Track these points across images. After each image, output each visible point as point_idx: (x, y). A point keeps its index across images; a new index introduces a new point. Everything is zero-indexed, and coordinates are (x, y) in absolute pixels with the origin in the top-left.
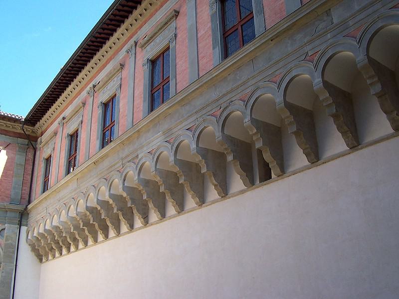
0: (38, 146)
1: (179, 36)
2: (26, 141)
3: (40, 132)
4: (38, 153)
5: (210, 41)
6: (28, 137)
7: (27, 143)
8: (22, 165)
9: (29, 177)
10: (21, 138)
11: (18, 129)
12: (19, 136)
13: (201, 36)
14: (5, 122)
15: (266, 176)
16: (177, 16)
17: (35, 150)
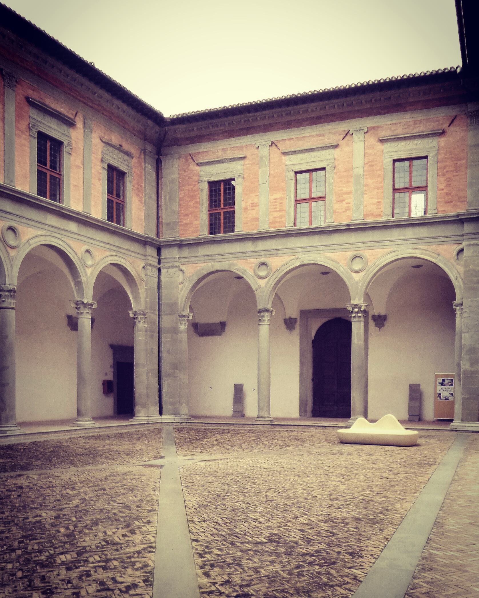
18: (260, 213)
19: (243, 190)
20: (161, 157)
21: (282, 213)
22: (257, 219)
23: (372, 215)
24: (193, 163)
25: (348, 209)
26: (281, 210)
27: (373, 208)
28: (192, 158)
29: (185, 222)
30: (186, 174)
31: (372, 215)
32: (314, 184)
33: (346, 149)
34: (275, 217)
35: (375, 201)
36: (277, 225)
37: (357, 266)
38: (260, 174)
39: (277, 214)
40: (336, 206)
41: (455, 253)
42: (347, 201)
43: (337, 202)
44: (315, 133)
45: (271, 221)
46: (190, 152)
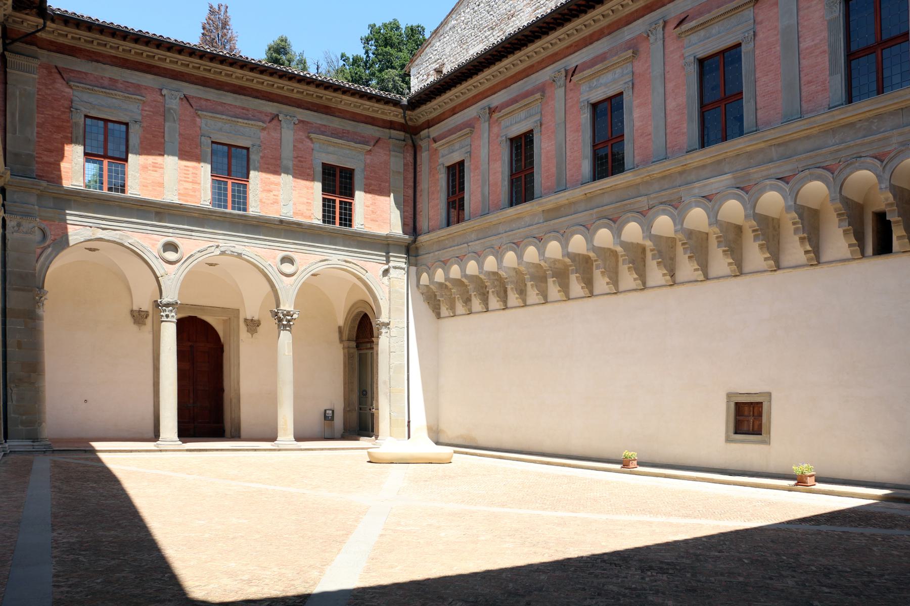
0: (423, 144)
2: (401, 135)
3: (423, 120)
4: (424, 156)
6: (403, 127)
7: (403, 138)
8: (399, 172)
9: (411, 192)
12: (391, 125)
14: (371, 104)
17: (415, 149)
18: (166, 178)
19: (141, 143)
20: (6, 53)
21: (196, 186)
22: (161, 185)
24: (61, 81)
28: (60, 73)
30: (48, 92)
32: (233, 161)
33: (275, 135)
34: (185, 189)
35: (306, 200)
37: (287, 268)
38: (166, 129)
39: (189, 186)
40: (264, 195)
42: (274, 193)
43: (264, 190)
44: (238, 104)
45: (181, 192)
46: (60, 65)
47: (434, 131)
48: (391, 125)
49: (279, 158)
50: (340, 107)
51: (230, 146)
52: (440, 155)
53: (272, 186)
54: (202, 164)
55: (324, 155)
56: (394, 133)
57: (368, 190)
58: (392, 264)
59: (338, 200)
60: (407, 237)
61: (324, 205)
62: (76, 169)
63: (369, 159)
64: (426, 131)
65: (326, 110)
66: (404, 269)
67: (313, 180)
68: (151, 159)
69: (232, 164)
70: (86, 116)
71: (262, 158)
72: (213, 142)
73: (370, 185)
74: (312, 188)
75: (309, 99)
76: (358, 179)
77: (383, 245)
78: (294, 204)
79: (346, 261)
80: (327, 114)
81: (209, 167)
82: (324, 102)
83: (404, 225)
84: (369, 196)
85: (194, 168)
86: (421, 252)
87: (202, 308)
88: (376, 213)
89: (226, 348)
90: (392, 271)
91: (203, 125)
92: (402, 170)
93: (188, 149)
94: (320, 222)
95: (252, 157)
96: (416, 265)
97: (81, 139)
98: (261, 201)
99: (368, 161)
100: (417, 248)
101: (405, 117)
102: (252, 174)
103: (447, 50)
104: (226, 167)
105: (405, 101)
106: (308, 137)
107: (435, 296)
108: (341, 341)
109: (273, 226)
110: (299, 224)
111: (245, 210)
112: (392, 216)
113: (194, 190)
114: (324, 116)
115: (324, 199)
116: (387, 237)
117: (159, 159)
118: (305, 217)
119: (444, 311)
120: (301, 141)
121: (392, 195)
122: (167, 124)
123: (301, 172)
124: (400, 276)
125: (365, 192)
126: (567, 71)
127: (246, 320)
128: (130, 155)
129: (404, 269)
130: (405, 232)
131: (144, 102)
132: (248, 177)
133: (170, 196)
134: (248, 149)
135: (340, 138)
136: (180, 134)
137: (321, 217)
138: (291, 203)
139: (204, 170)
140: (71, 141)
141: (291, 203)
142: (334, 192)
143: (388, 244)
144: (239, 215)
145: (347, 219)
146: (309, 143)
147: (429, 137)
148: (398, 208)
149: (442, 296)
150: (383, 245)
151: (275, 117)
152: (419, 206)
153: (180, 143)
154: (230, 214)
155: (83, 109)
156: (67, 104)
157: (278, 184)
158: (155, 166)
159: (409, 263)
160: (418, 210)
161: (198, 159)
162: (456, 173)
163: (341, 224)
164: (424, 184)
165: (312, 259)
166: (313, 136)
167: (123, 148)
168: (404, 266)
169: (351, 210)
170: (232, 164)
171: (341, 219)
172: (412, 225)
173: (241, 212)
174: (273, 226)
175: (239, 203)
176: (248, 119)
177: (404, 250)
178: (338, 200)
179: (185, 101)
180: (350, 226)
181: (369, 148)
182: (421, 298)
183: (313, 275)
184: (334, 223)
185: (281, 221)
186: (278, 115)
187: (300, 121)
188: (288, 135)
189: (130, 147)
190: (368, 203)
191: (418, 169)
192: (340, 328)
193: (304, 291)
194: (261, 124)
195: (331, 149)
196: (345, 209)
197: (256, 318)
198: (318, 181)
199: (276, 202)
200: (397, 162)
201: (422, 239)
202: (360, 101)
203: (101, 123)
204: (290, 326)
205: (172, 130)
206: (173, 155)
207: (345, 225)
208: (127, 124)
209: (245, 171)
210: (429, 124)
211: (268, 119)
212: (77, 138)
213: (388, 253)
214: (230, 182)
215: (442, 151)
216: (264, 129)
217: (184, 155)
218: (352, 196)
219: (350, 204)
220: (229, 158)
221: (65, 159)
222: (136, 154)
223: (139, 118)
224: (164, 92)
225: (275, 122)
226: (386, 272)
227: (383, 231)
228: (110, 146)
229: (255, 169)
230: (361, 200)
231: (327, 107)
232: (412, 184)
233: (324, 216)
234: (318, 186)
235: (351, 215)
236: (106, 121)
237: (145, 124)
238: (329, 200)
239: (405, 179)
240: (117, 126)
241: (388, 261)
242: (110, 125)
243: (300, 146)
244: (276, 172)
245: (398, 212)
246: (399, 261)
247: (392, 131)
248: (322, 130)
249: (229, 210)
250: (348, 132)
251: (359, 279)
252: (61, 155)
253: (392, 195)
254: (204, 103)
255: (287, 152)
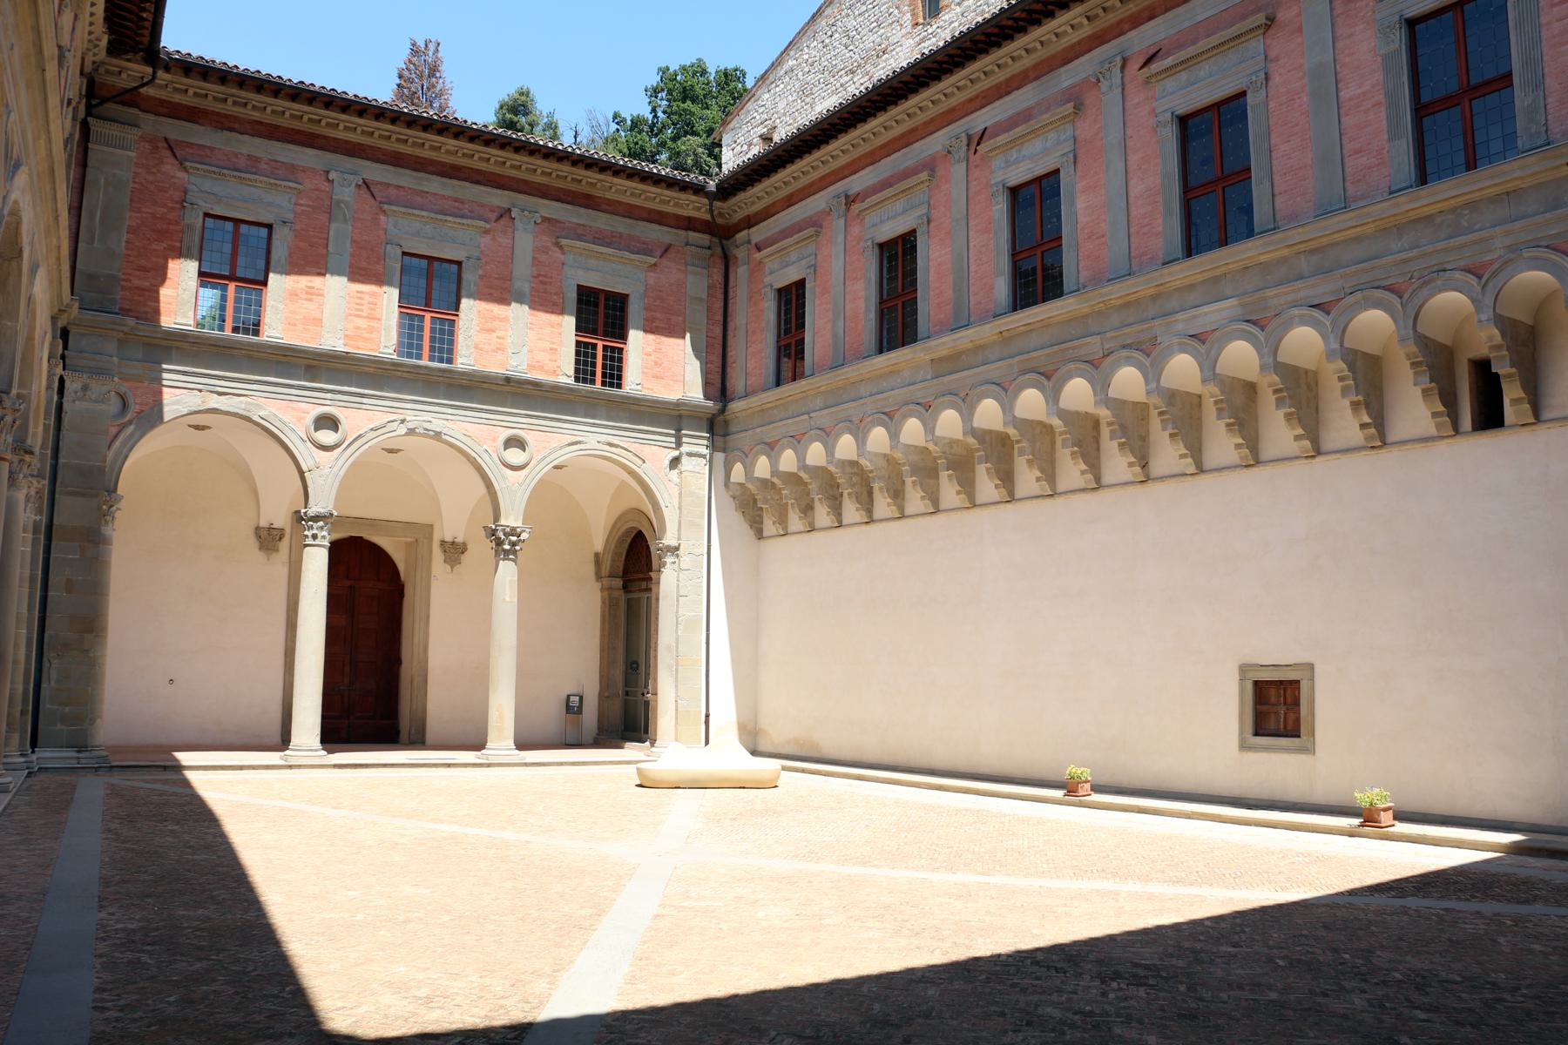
0: (740, 253)
1: (1276, 80)
2: (704, 239)
4: (741, 273)
5: (1380, 118)
6: (708, 227)
7: (707, 243)
8: (701, 299)
9: (718, 331)
10: (695, 230)
11: (693, 207)
12: (689, 224)
13: (1350, 99)
15: (1490, 417)
16: (1268, 27)
17: (727, 261)
19: (290, 255)
22: (318, 322)
23: (541, 368)
25: (501, 349)
26: (370, 318)
27: (543, 357)
29: (137, 282)
31: (541, 368)
32: (436, 284)
33: (503, 240)
35: (548, 345)
36: (361, 344)
37: (515, 456)
41: (667, 462)
42: (499, 333)
47: (758, 233)
48: (689, 224)
49: (509, 278)
50: (608, 196)
51: (431, 259)
52: (767, 271)
53: (496, 323)
54: (385, 288)
55: (580, 272)
56: (693, 236)
57: (650, 328)
58: (685, 448)
59: (600, 345)
60: (710, 403)
61: (578, 353)
62: (184, 298)
63: (652, 278)
64: (745, 232)
65: (587, 201)
66: (704, 456)
67: (562, 312)
68: (303, 281)
69: (433, 288)
70: (206, 215)
71: (481, 277)
72: (404, 253)
73: (653, 319)
74: (560, 325)
75: (560, 184)
76: (634, 309)
77: (669, 417)
78: (530, 351)
79: (611, 445)
80: (587, 207)
81: (395, 293)
82: (583, 188)
83: (707, 384)
84: (651, 337)
85: (373, 294)
86: (733, 428)
87: (372, 523)
88: (662, 365)
89: (408, 591)
90: (685, 460)
91: (390, 227)
92: (704, 296)
93: (364, 264)
94: (571, 381)
95: (466, 276)
96: (724, 450)
97: (196, 251)
98: (476, 347)
99: (651, 282)
100: (726, 423)
101: (711, 211)
102: (466, 303)
103: (781, 105)
104: (423, 293)
105: (712, 185)
106: (557, 244)
107: (755, 501)
108: (599, 577)
109: (494, 387)
110: (536, 384)
111: (450, 361)
112: (688, 368)
113: (370, 330)
114: (582, 210)
115: (578, 343)
116: (678, 404)
117: (317, 281)
118: (547, 372)
119: (769, 527)
120: (545, 251)
121: (688, 336)
122: (334, 226)
123: (543, 300)
124: (698, 469)
125: (646, 331)
126: (969, 138)
127: (443, 543)
128: (271, 275)
129: (704, 456)
130: (707, 397)
131: (300, 192)
132: (457, 309)
133: (332, 341)
134: (459, 263)
135: (608, 245)
136: (353, 241)
137: (572, 372)
138: (525, 350)
139: (389, 297)
140: (180, 254)
141: (525, 350)
142: (594, 332)
143: (680, 416)
144: (440, 370)
145: (614, 376)
146: (557, 253)
147: (749, 242)
148: (697, 357)
149: (766, 501)
150: (669, 417)
151: (505, 213)
152: (731, 353)
153: (352, 255)
154: (426, 367)
155: (201, 203)
156: (177, 195)
157: (505, 320)
158: (311, 293)
159: (713, 447)
160: (730, 360)
161: (380, 280)
162: (792, 300)
163: (604, 384)
164: (739, 318)
165: (556, 441)
166: (564, 242)
167: (261, 264)
168: (705, 451)
169: (620, 360)
170: (433, 288)
171: (604, 375)
172: (719, 385)
173: (444, 365)
174: (494, 387)
175: (441, 350)
176: (462, 217)
177: (705, 425)
178: (600, 345)
179: (364, 189)
180: (619, 386)
181: (653, 260)
182: (730, 505)
183: (556, 467)
184: (593, 382)
185: (508, 380)
186: (509, 210)
187: (545, 219)
188: (525, 241)
189: (273, 263)
190: (650, 349)
191: (731, 294)
192: (597, 555)
193: (545, 495)
194: (482, 223)
195: (593, 262)
196: (612, 359)
197: (459, 540)
198: (570, 314)
199: (501, 349)
200: (697, 283)
201: (736, 406)
202: (641, 186)
203: (229, 226)
204: (515, 552)
205: (340, 235)
206: (340, 274)
207: (612, 385)
208: (270, 227)
209: (453, 296)
210: (750, 222)
211: (494, 216)
212: (189, 249)
213: (679, 430)
214: (428, 316)
215: (770, 265)
216: (487, 232)
217: (360, 272)
218: (623, 337)
219: (621, 350)
220: (429, 277)
221: (168, 282)
222: (281, 273)
223: (290, 216)
224: (332, 175)
225: (504, 221)
226: (675, 462)
227: (672, 395)
228: (241, 261)
229: (469, 296)
230: (638, 344)
231: (589, 197)
232: (721, 318)
233: (577, 371)
234: (570, 322)
235: (620, 369)
236: (237, 222)
237: (298, 227)
238: (586, 345)
239: (709, 309)
240: (254, 229)
241: (679, 444)
242: (244, 228)
243: (542, 258)
244: (503, 300)
245: (697, 364)
246: (696, 443)
247: (691, 234)
248: (579, 234)
249: (425, 362)
250: (621, 235)
251: (632, 473)
252: (162, 277)
253: (688, 336)
254: (393, 191)
255: (522, 268)
